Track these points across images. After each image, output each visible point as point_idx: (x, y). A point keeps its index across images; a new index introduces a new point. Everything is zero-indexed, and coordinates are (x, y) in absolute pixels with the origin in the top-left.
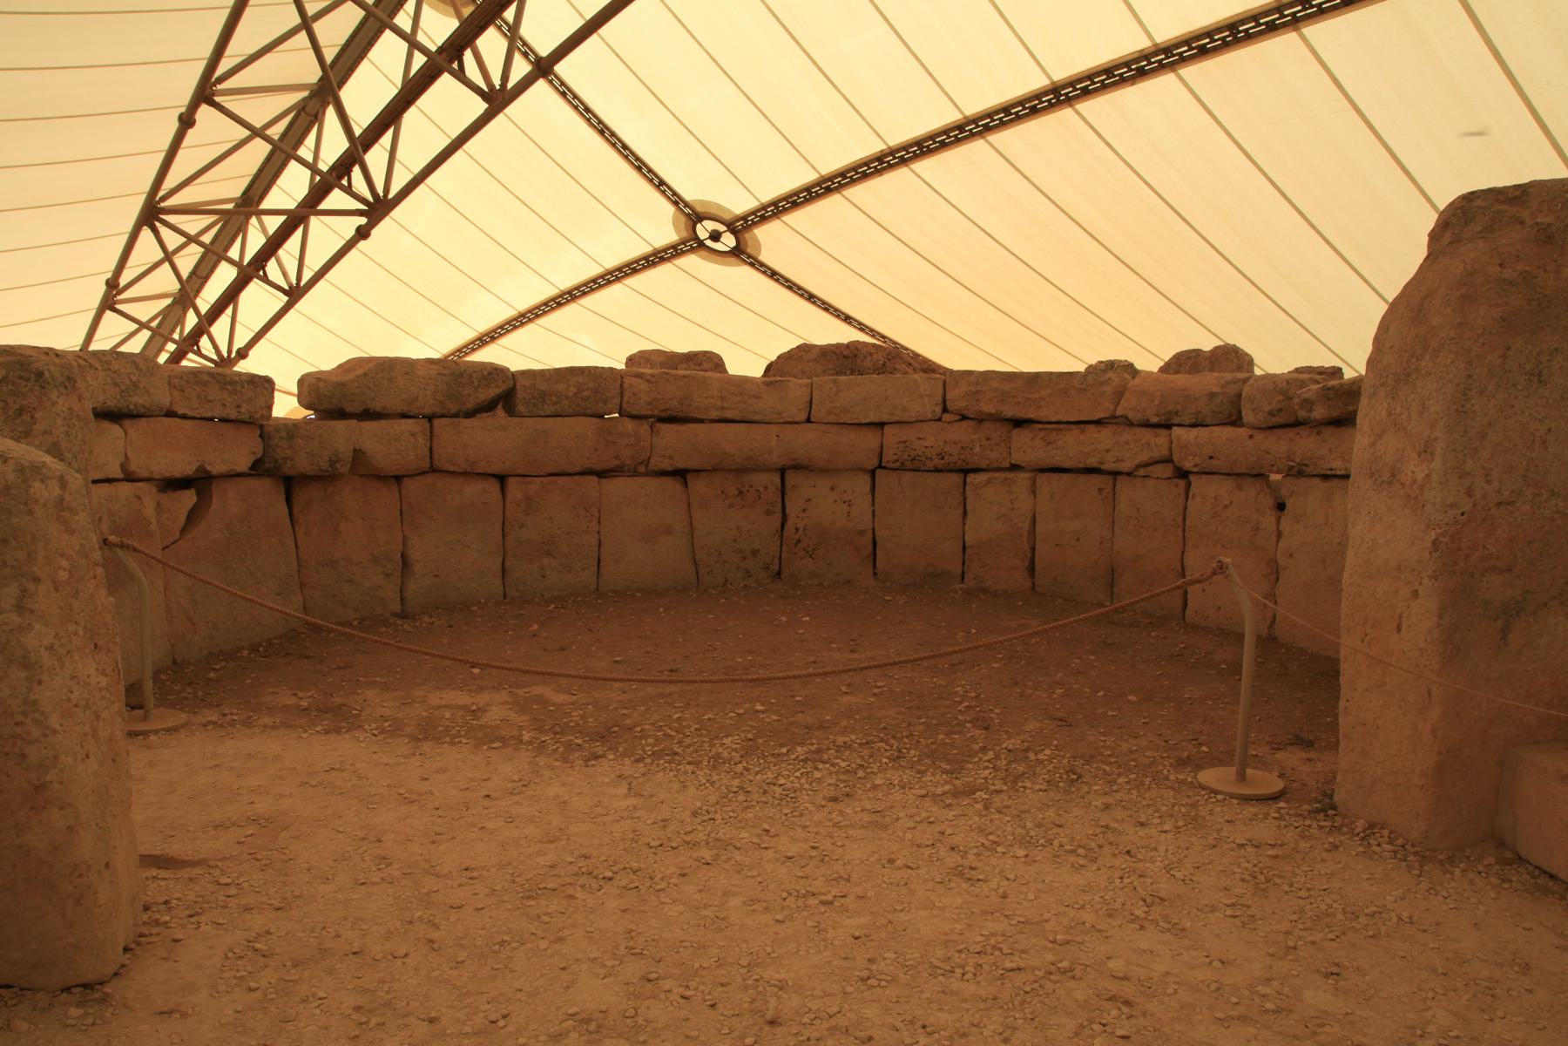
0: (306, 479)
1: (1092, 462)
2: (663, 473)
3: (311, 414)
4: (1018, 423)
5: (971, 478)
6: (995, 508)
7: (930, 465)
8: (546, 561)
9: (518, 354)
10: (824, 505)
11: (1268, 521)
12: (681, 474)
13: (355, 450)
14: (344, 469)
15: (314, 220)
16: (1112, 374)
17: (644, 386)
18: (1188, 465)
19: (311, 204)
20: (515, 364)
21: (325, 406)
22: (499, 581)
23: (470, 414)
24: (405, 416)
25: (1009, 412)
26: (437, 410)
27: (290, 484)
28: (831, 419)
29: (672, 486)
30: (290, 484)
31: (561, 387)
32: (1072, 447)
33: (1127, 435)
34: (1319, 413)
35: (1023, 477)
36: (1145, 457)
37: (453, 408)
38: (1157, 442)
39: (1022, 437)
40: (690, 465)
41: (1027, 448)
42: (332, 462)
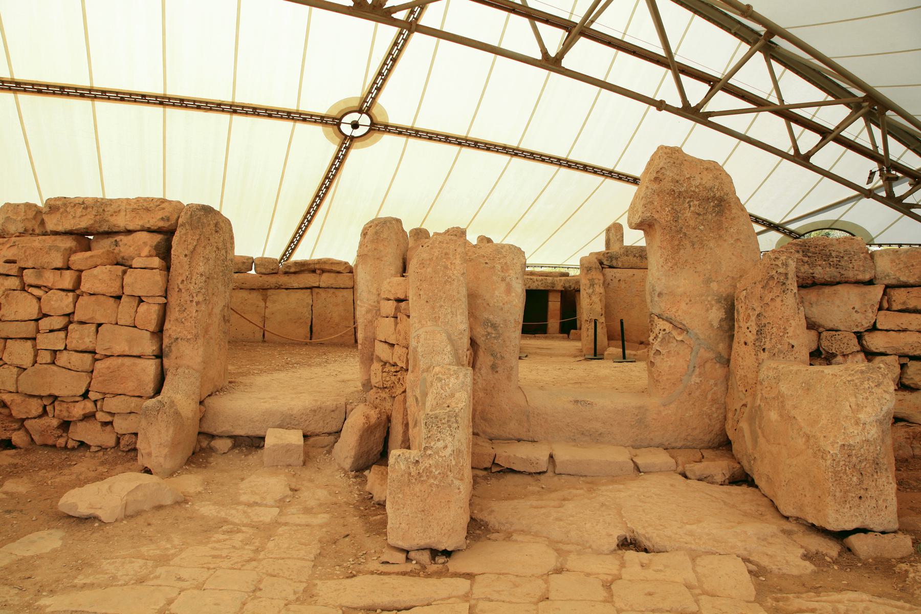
34: (293, 270)
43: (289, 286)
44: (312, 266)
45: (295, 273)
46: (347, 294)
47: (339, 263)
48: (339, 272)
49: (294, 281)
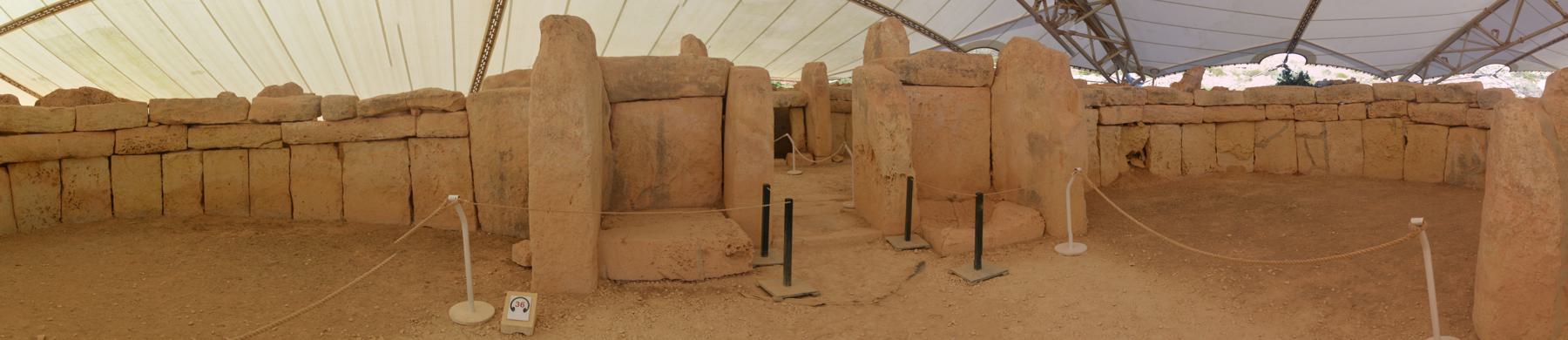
1: (237, 144)
4: (189, 126)
11: (337, 165)
16: (227, 99)
18: (291, 141)
32: (224, 137)
33: (256, 129)
34: (371, 112)
35: (196, 154)
38: (274, 131)
41: (197, 138)
44: (402, 104)
45: (377, 116)
46: (459, 146)
47: (443, 95)
48: (445, 111)
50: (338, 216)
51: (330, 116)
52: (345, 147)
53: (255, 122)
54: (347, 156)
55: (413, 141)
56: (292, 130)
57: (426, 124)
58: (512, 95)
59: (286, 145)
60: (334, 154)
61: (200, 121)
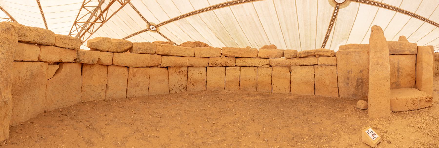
0: (87, 65)
1: (253, 65)
2: (163, 67)
3: (89, 49)
4: (236, 58)
5: (227, 68)
6: (232, 74)
7: (219, 66)
8: (137, 88)
9: (133, 40)
10: (197, 74)
12: (167, 68)
13: (99, 59)
14: (95, 63)
15: (95, 23)
17: (161, 48)
18: (272, 65)
19: (95, 21)
20: (133, 42)
21: (93, 47)
22: (125, 93)
23: (122, 52)
24: (107, 52)
25: (236, 56)
26: (115, 51)
27: (83, 65)
28: (199, 56)
29: (165, 70)
30: (83, 65)
31: (143, 47)
32: (249, 62)
33: (260, 60)
34: (303, 56)
35: (238, 68)
36: (264, 64)
37: (119, 50)
38: (267, 61)
39: (238, 60)
40: (170, 66)
41: (239, 62)
42: (93, 61)
43: (302, 64)
44: (313, 54)
45: (304, 57)
48: (328, 56)
49: (303, 62)
50: (289, 92)
51: (288, 57)
52: (292, 68)
53: (260, 58)
54: (293, 71)
55: (316, 66)
56: (273, 61)
57: (321, 60)
58: (353, 52)
59: (271, 66)
60: (288, 70)
61: (240, 56)
